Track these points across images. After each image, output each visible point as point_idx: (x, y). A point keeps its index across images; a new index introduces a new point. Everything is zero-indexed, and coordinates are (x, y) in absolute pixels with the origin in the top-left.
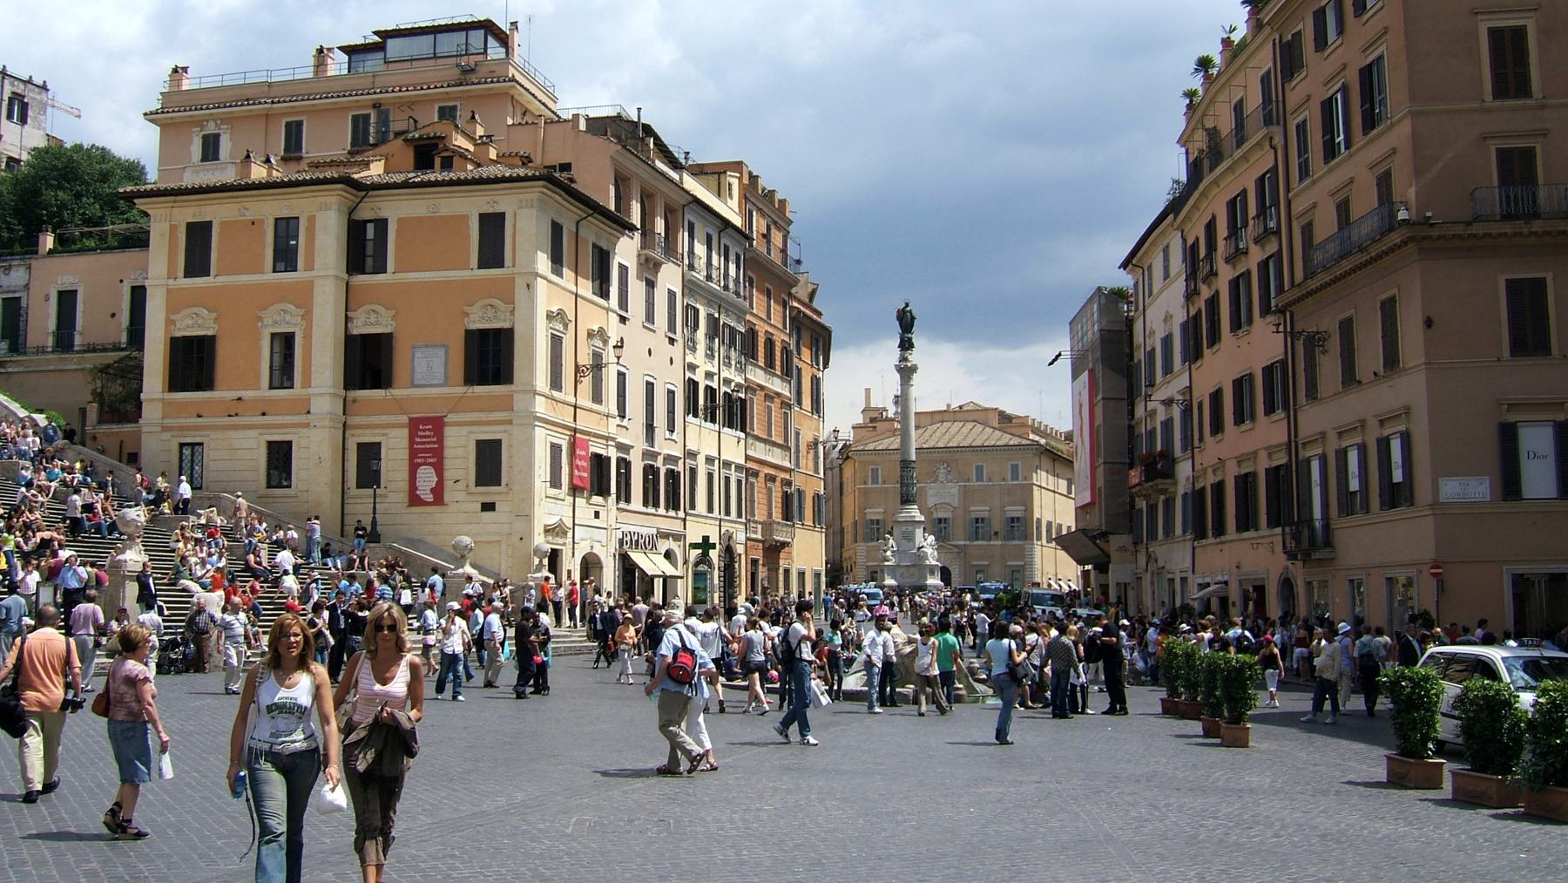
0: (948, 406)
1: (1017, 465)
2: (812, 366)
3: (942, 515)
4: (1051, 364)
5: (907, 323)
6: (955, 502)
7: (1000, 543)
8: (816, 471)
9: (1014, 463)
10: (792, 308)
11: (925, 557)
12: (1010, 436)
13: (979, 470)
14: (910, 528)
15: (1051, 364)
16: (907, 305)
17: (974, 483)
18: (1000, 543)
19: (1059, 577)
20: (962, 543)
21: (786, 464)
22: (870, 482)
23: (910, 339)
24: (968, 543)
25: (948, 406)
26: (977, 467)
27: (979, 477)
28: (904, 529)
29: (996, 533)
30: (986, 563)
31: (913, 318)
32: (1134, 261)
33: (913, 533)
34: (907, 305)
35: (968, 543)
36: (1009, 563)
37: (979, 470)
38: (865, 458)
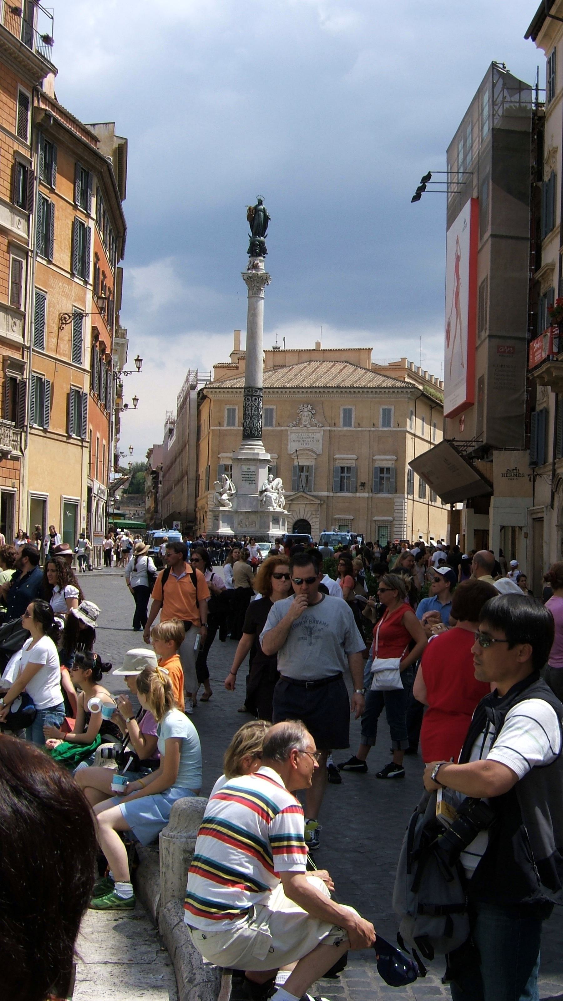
0: (318, 344)
1: (389, 410)
2: (75, 207)
3: (303, 462)
4: (417, 198)
5: (259, 225)
6: (319, 448)
7: (366, 495)
8: (77, 355)
9: (386, 407)
10: (37, 110)
11: (269, 502)
12: (383, 378)
13: (348, 413)
14: (253, 468)
15: (417, 198)
16: (260, 202)
18: (366, 495)
19: (431, 535)
20: (325, 494)
21: (16, 337)
22: (225, 423)
23: (262, 243)
24: (331, 494)
25: (318, 344)
26: (345, 410)
27: (347, 422)
28: (245, 468)
29: (363, 485)
30: (352, 517)
31: (267, 219)
32: (553, 12)
34: (260, 202)
35: (331, 494)
36: (376, 518)
37: (348, 413)
38: (222, 396)
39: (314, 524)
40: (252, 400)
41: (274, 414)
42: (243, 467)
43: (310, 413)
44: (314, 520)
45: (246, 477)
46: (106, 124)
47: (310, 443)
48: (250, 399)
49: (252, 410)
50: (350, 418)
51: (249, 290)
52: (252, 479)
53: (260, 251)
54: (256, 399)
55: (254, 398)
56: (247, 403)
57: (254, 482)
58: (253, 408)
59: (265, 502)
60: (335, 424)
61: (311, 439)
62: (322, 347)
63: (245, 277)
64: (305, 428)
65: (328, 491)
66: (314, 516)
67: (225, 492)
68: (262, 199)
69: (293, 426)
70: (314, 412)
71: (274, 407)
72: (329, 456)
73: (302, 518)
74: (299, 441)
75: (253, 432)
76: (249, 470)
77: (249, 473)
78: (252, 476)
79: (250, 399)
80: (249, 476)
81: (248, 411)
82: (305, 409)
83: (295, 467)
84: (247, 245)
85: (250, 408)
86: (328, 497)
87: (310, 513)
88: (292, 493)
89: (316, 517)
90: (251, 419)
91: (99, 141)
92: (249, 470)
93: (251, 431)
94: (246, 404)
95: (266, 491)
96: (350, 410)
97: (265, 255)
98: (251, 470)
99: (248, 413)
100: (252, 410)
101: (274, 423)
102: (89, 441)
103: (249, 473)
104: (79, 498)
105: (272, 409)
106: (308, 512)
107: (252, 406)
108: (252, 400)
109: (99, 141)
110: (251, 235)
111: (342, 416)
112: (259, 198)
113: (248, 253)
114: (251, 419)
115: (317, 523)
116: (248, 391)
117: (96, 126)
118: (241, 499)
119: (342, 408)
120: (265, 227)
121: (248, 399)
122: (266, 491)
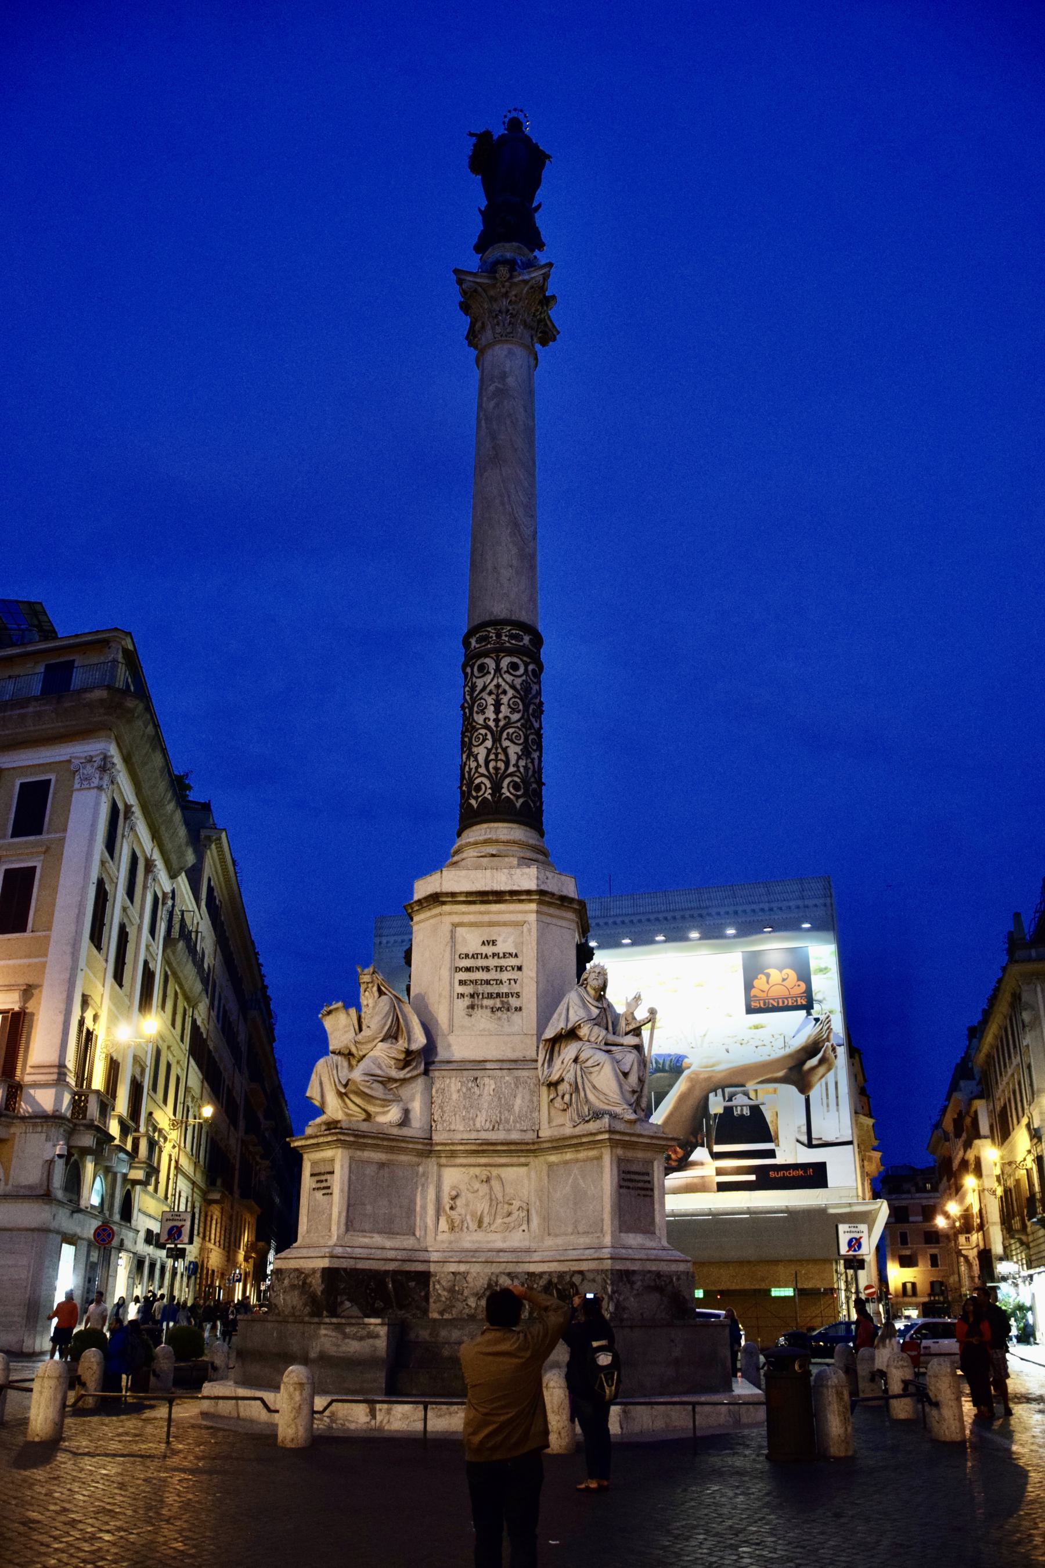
40: (498, 669)
45: (475, 982)
52: (504, 989)
55: (505, 662)
56: (480, 683)
57: (513, 1002)
58: (505, 699)
76: (489, 950)
77: (492, 962)
78: (505, 976)
79: (490, 663)
80: (492, 975)
81: (483, 712)
85: (490, 700)
92: (489, 950)
93: (496, 787)
94: (473, 687)
98: (500, 948)
99: (479, 719)
103: (492, 962)
107: (501, 692)
114: (497, 740)
121: (482, 668)
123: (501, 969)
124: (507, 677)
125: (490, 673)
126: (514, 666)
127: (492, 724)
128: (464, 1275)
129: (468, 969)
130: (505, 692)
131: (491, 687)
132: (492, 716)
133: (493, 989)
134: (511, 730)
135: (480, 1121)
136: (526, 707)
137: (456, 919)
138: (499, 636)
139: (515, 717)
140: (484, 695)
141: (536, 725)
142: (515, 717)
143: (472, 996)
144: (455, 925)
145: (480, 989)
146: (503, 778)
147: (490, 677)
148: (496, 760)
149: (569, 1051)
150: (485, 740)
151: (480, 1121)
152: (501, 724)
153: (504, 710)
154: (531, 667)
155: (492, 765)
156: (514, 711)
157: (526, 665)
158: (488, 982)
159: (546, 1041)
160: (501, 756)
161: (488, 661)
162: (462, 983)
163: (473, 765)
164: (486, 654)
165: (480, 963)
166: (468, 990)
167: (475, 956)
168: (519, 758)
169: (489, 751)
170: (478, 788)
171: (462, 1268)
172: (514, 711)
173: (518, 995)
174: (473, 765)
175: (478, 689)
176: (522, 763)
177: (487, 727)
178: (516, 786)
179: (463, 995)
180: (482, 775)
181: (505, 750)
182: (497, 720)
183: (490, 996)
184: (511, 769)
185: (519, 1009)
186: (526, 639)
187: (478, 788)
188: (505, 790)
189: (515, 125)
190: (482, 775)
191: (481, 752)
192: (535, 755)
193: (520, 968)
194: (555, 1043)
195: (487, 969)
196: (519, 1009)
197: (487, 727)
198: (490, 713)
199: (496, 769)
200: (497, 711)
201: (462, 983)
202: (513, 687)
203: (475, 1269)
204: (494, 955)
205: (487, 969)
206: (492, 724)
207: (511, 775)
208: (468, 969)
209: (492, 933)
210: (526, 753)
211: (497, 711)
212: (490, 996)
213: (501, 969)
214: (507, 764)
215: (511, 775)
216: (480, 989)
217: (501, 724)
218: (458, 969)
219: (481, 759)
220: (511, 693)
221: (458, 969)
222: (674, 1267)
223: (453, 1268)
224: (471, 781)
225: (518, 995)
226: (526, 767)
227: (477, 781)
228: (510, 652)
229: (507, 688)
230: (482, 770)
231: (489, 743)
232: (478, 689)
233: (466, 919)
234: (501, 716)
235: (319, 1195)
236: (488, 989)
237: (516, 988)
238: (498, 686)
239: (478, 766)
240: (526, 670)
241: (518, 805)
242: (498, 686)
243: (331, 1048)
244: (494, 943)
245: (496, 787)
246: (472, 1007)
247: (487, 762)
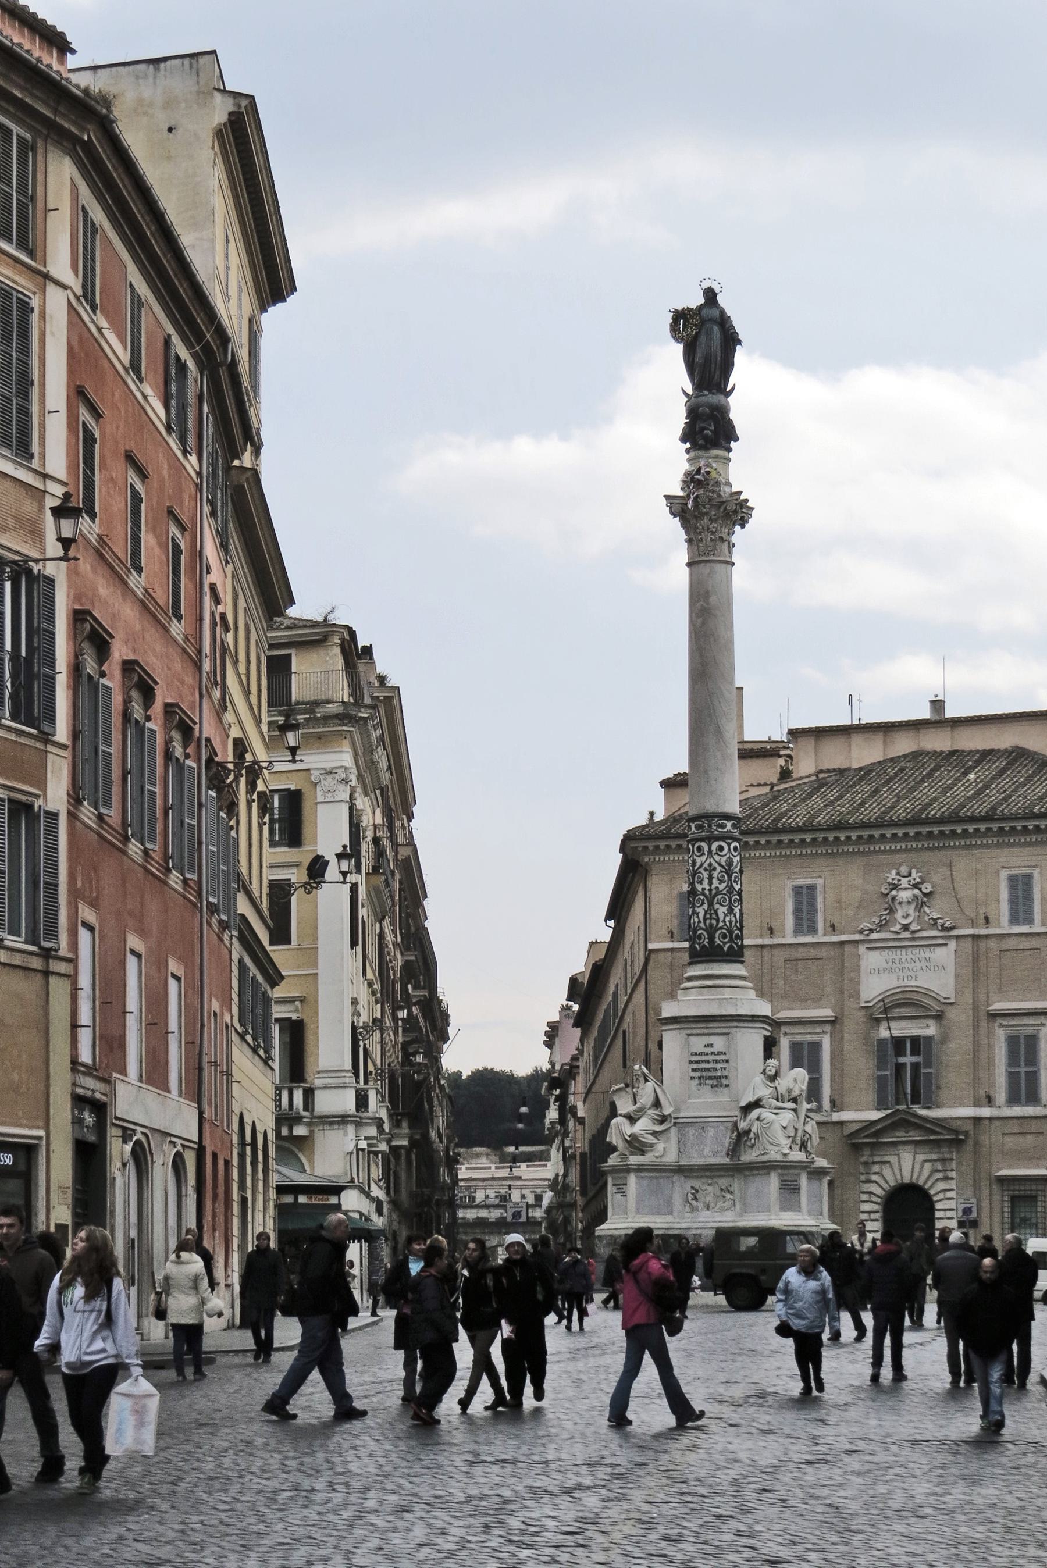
0: (937, 705)
5: (708, 359)
14: (719, 1043)
17: (1003, 925)
25: (937, 705)
26: (1013, 880)
28: (698, 1044)
31: (730, 340)
33: (723, 1058)
39: (941, 1196)
40: (710, 852)
41: (820, 899)
42: (693, 1039)
43: (916, 891)
44: (941, 1186)
45: (701, 1070)
46: (192, 56)
47: (920, 973)
48: (706, 848)
49: (710, 878)
50: (1029, 899)
51: (690, 541)
52: (719, 1074)
53: (715, 432)
54: (721, 848)
56: (699, 861)
57: (724, 1082)
58: (715, 874)
59: (757, 1136)
60: (987, 919)
61: (924, 964)
62: (950, 713)
63: (677, 508)
64: (907, 935)
65: (977, 1104)
66: (940, 1175)
67: (642, 1111)
68: (717, 289)
69: (871, 931)
70: (927, 888)
71: (820, 882)
72: (975, 1007)
73: (907, 1180)
74: (890, 971)
75: (718, 941)
77: (711, 1058)
78: (719, 1066)
79: (706, 848)
81: (701, 882)
82: (904, 883)
83: (882, 1042)
84: (679, 419)
85: (706, 875)
86: (977, 1120)
87: (928, 1166)
88: (875, 1115)
89: (947, 1178)
90: (711, 904)
91: (73, 52)
92: (709, 1050)
93: (711, 938)
95: (756, 1104)
96: (1028, 878)
97: (733, 444)
98: (715, 1049)
99: (699, 887)
100: (710, 878)
101: (820, 925)
102: (70, 955)
103: (711, 1058)
104: (42, 1133)
105: (812, 888)
106: (922, 1167)
107: (711, 869)
108: (710, 852)
109: (73, 52)
110: (690, 391)
111: (1004, 894)
112: (706, 285)
113: (684, 439)
114: (711, 904)
115: (949, 1194)
116: (698, 827)
117: (162, 65)
118: (691, 1131)
119: (1004, 874)
120: (727, 366)
121: (699, 849)
122: (756, 1104)
123: (716, 1062)
124: (716, 857)
125: (703, 854)
126: (721, 848)
127: (707, 892)
128: (700, 1235)
129: (697, 1062)
130: (715, 869)
131: (706, 865)
132: (707, 887)
133: (713, 1074)
134: (720, 897)
135: (707, 1151)
136: (730, 877)
137: (689, 1032)
138: (710, 826)
139: (722, 887)
140: (702, 870)
141: (737, 887)
142: (722, 887)
143: (699, 1078)
144: (689, 1035)
145: (704, 1074)
146: (716, 930)
147: (704, 858)
148: (711, 918)
149: (755, 1113)
150: (703, 903)
151: (707, 1151)
152: (714, 892)
153: (715, 882)
154: (732, 846)
155: (708, 922)
156: (721, 882)
157: (729, 845)
158: (709, 1070)
159: (742, 1108)
160: (714, 916)
161: (703, 844)
162: (694, 1070)
163: (696, 920)
164: (702, 840)
165: (704, 1058)
166: (698, 1074)
167: (701, 1054)
168: (726, 915)
169: (706, 912)
170: (700, 937)
171: (699, 1232)
172: (721, 882)
173: (726, 1077)
174: (696, 920)
175: (698, 864)
176: (728, 919)
177: (703, 894)
178: (724, 936)
179: (693, 1078)
180: (702, 929)
181: (716, 912)
182: (710, 890)
183: (711, 1078)
184: (721, 924)
185: (727, 1086)
186: (729, 825)
187: (700, 937)
188: (717, 940)
189: (710, 295)
190: (702, 929)
191: (701, 911)
192: (737, 910)
193: (727, 1061)
194: (747, 1109)
195: (708, 1062)
196: (727, 1086)
197: (703, 894)
198: (706, 885)
199: (711, 925)
200: (710, 883)
201: (694, 1070)
202: (720, 865)
203: (705, 1232)
204: (712, 1053)
205: (708, 1062)
206: (707, 892)
207: (721, 928)
208: (697, 1062)
209: (712, 1039)
210: (731, 911)
211: (710, 883)
212: (711, 1078)
213: (716, 1062)
214: (718, 921)
215: (721, 928)
216: (704, 1074)
217: (714, 892)
218: (691, 1062)
219: (701, 916)
220: (719, 869)
221: (691, 1062)
222: (808, 1229)
223: (694, 1232)
224: (695, 931)
225: (726, 1077)
226: (730, 922)
227: (700, 932)
228: (718, 839)
229: (716, 865)
230: (702, 925)
231: (706, 906)
232: (698, 864)
233: (694, 1031)
234: (713, 886)
235: (618, 1196)
236: (709, 1074)
237: (725, 1073)
238: (710, 865)
239: (699, 922)
240: (729, 849)
241: (725, 949)
242: (710, 865)
243: (619, 1112)
244: (711, 1045)
245: (711, 938)
246: (700, 1084)
247: (705, 919)
